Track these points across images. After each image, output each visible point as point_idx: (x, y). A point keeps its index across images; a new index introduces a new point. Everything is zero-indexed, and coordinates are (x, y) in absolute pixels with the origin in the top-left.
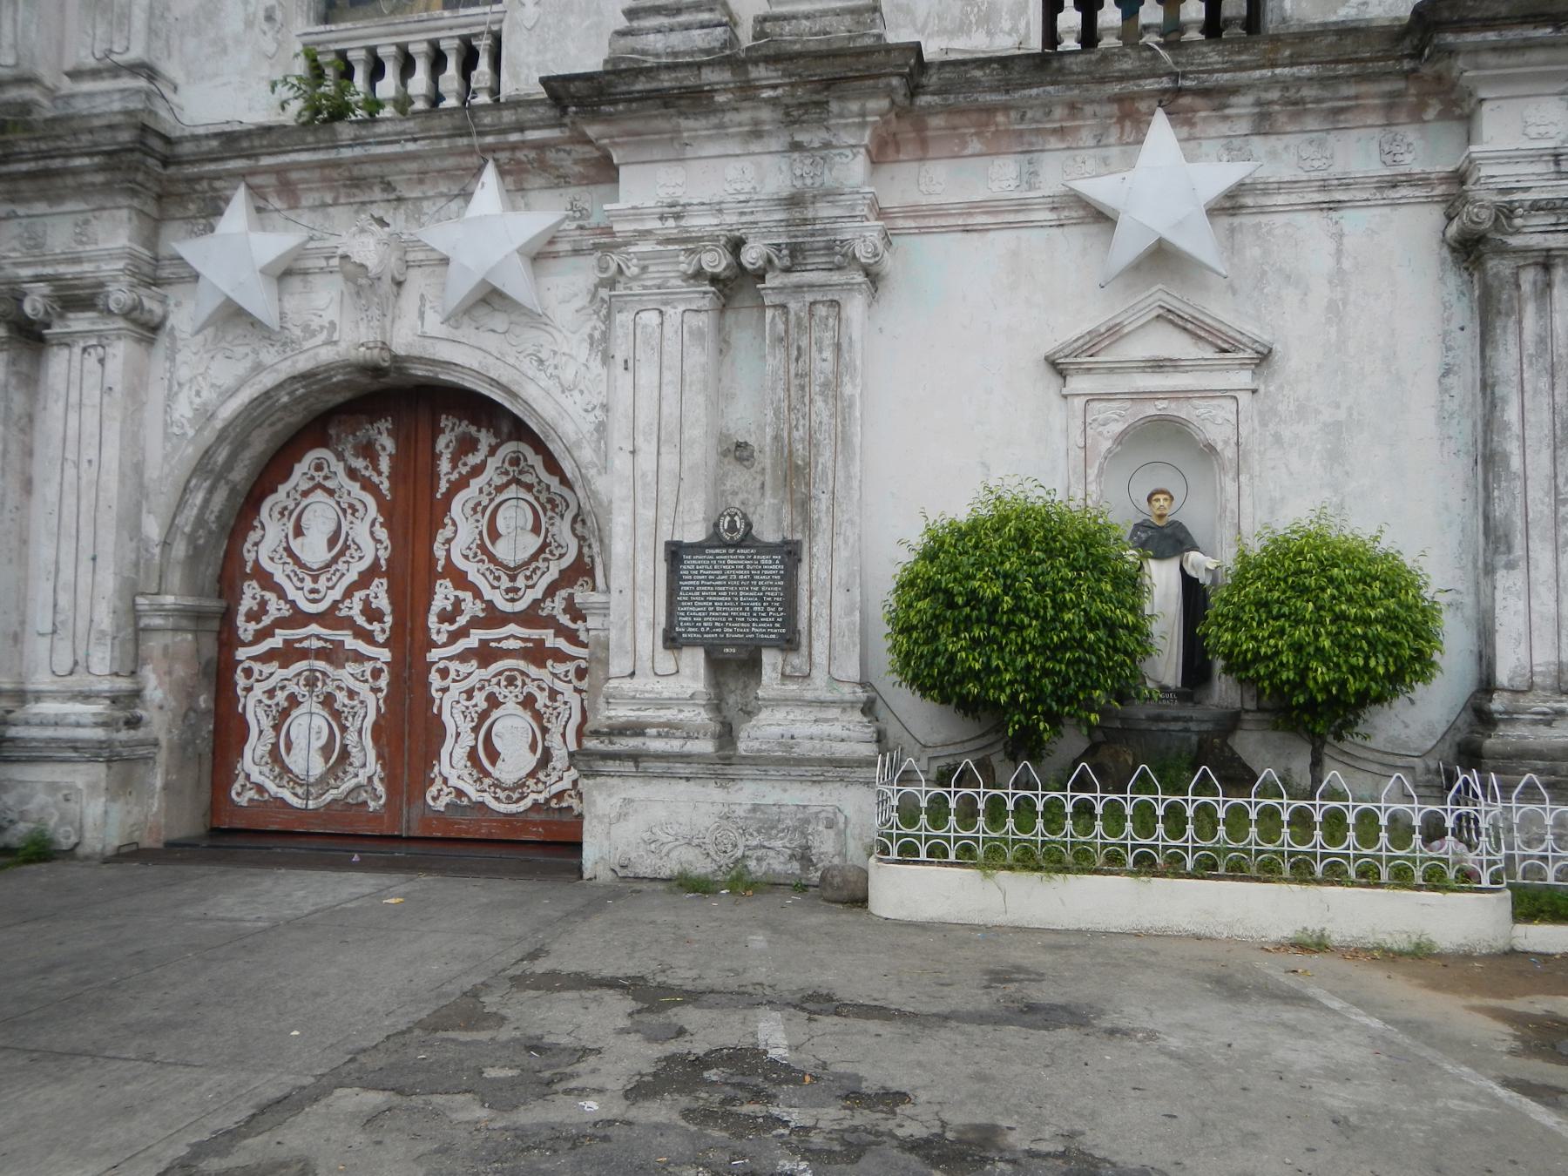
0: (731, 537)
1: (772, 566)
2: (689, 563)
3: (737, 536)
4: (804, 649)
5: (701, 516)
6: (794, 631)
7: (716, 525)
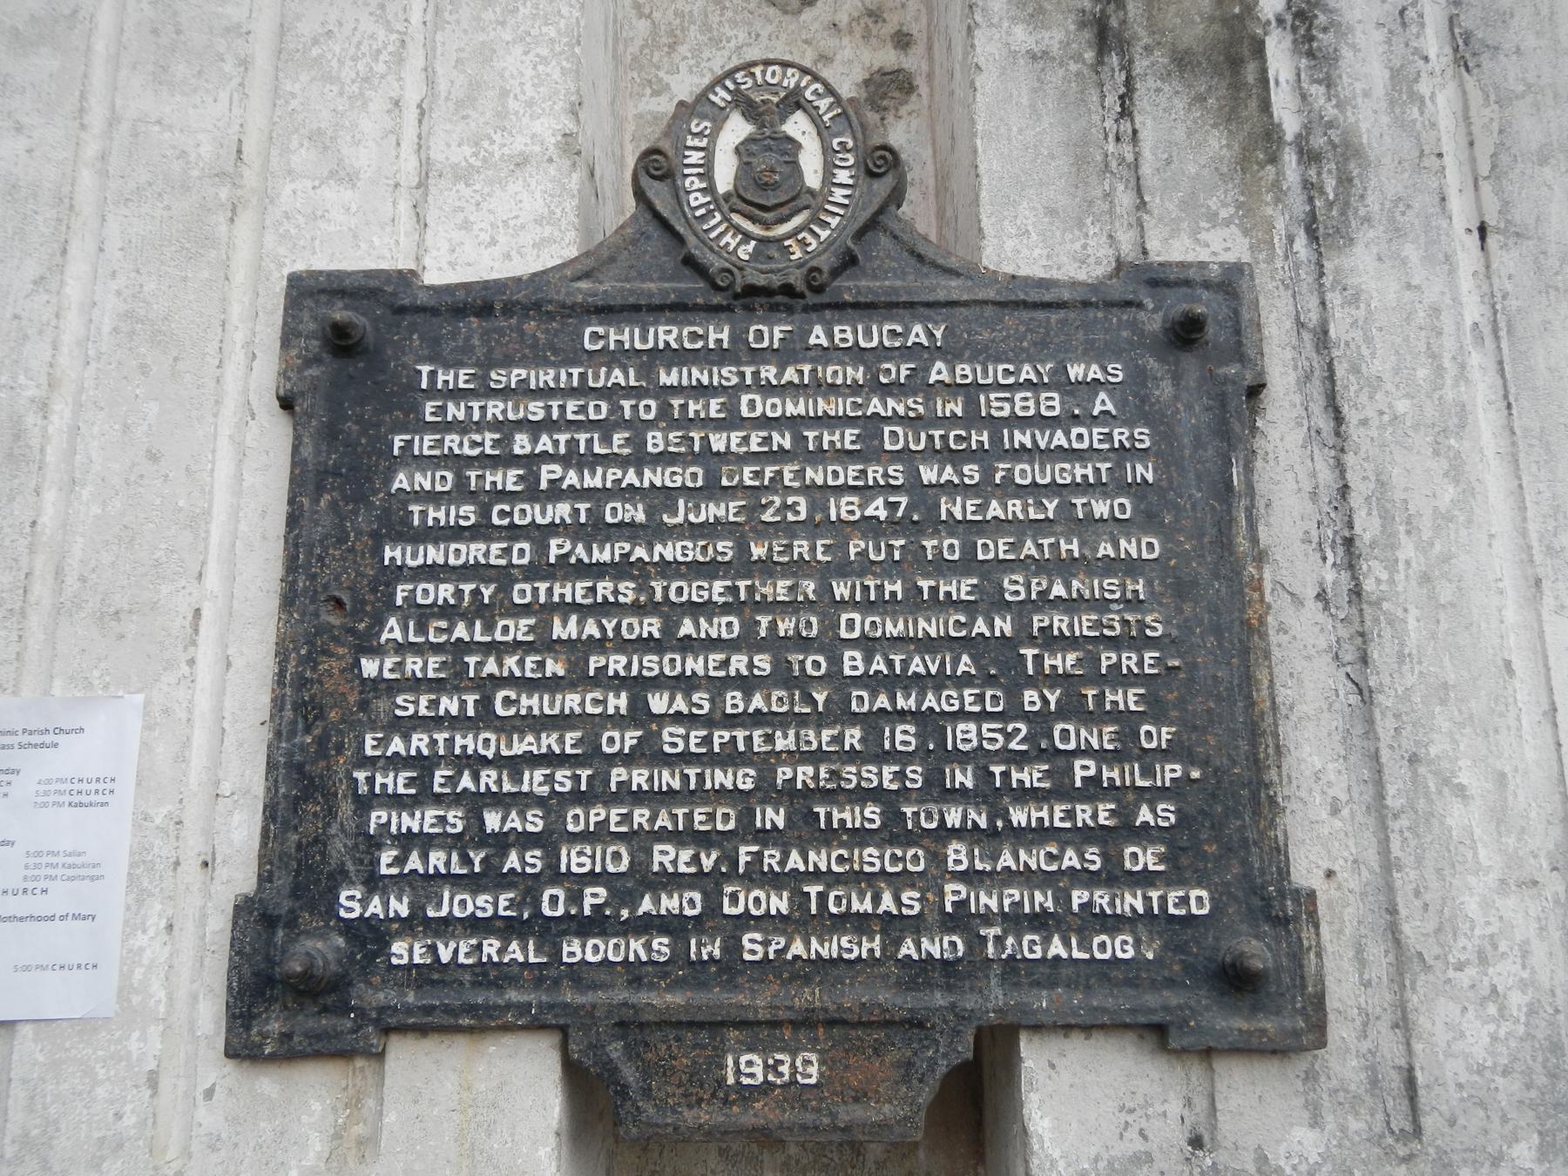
0: (763, 254)
1: (1073, 432)
2: (459, 417)
3: (807, 242)
4: (1347, 1049)
5: (548, 127)
6: (1282, 909)
7: (657, 167)
